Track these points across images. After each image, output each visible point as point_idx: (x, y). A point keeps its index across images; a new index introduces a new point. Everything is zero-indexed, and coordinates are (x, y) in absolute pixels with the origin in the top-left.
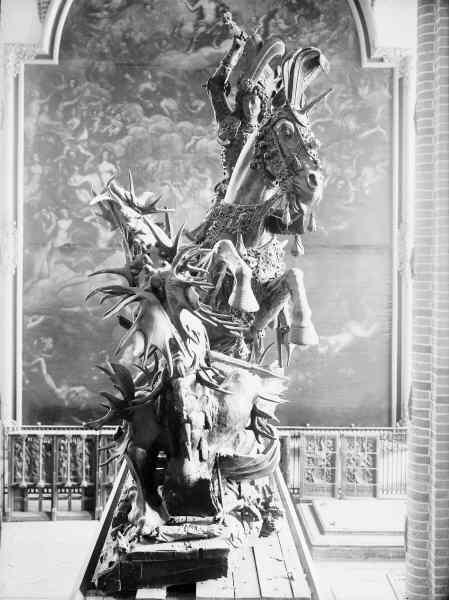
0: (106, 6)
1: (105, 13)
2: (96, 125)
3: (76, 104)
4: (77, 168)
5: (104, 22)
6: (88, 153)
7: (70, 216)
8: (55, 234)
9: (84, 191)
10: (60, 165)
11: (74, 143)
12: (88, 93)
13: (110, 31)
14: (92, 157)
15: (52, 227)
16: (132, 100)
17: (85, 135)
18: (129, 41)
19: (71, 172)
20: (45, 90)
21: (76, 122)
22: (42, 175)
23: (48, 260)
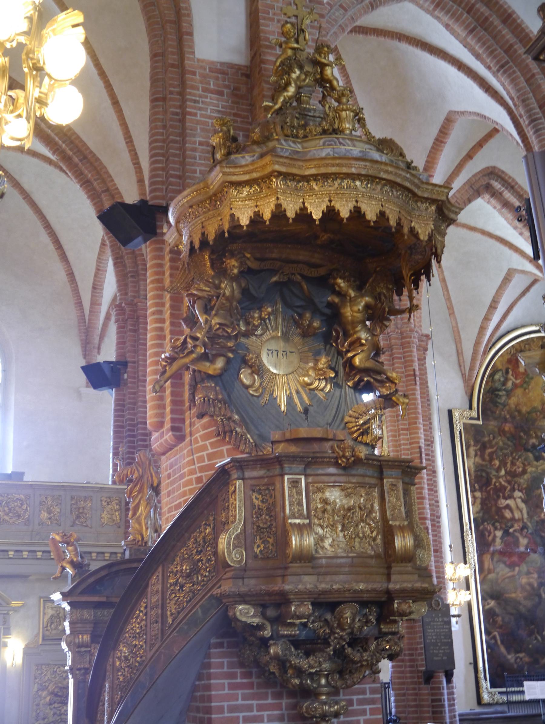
0: (504, 388)
1: (504, 393)
2: (509, 465)
3: (495, 451)
4: (501, 495)
5: (504, 398)
6: (506, 484)
7: (501, 528)
8: (494, 540)
9: (507, 511)
10: (491, 492)
11: (498, 477)
12: (501, 443)
13: (508, 404)
14: (509, 487)
15: (492, 535)
16: (527, 450)
17: (503, 472)
18: (519, 412)
19: (498, 497)
20: (476, 442)
21: (497, 463)
22: (482, 499)
23: (492, 560)
